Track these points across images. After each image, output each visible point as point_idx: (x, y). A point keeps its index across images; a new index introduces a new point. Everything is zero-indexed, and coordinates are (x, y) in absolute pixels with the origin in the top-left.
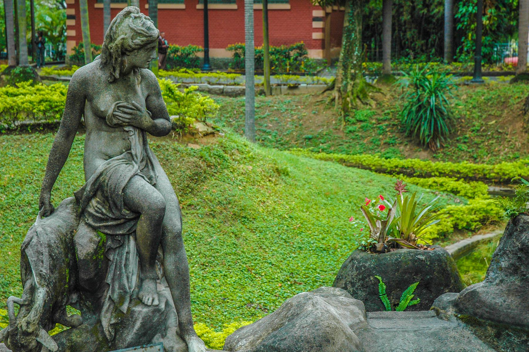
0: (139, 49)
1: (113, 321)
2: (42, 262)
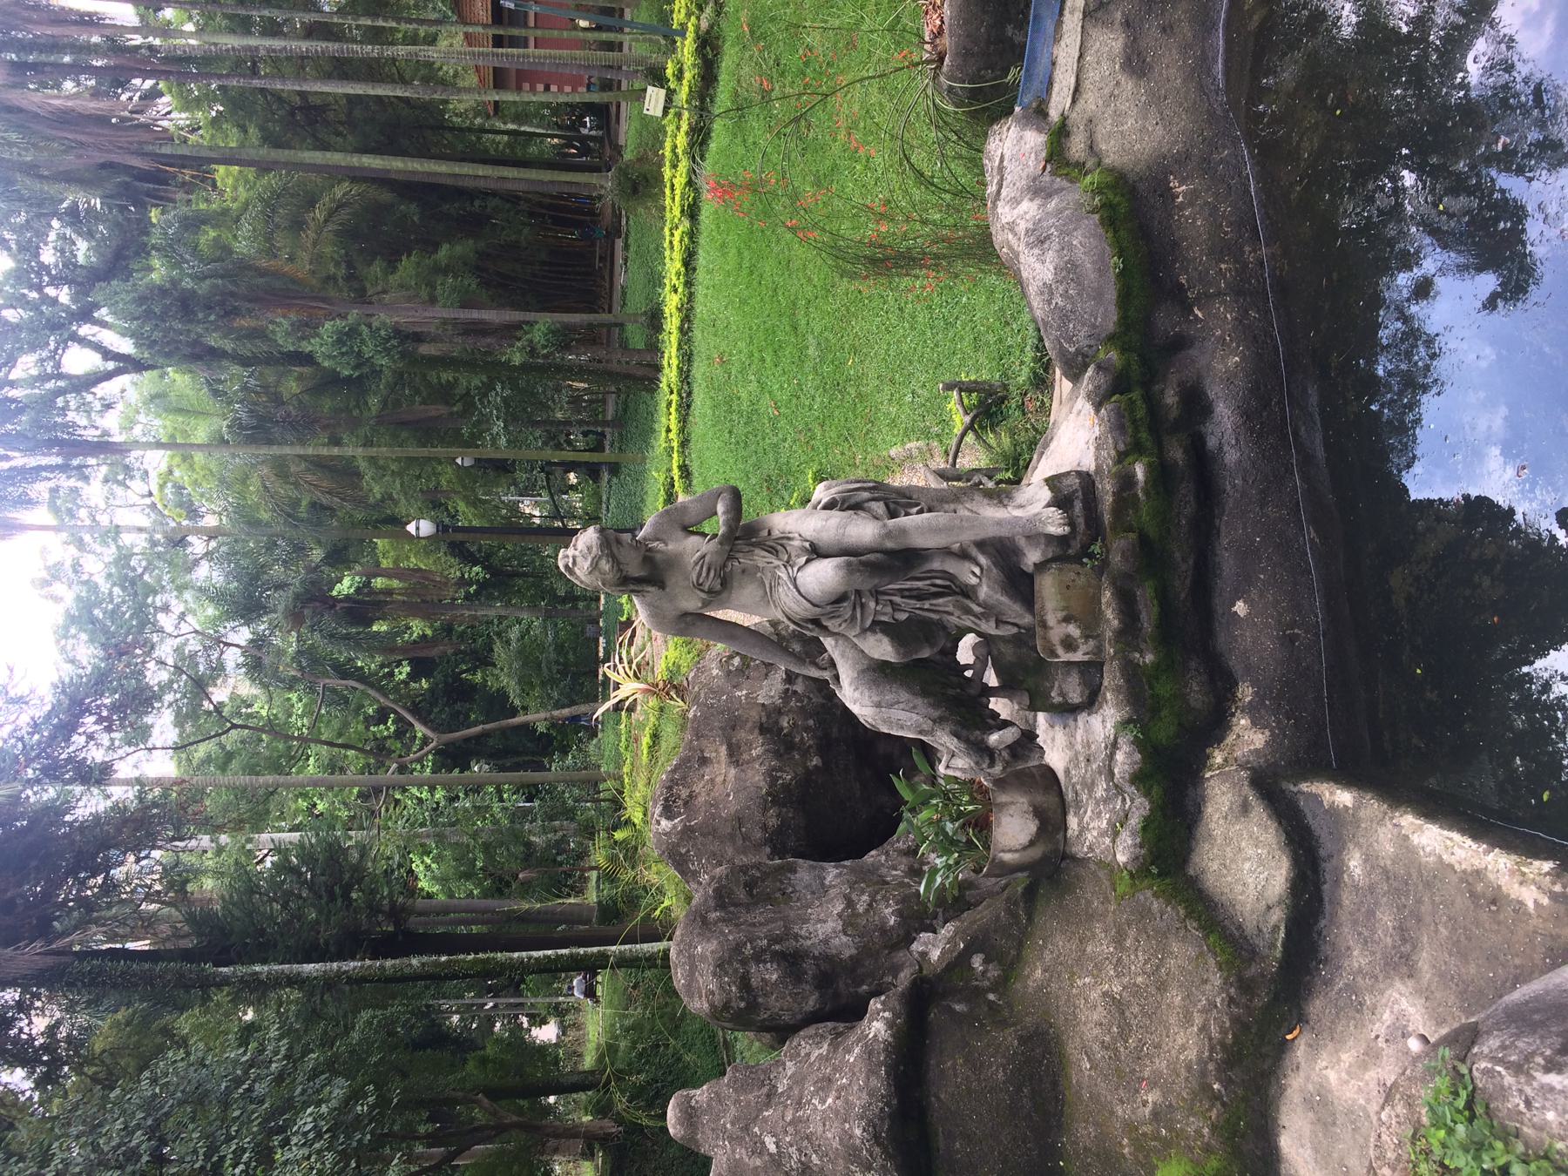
0: (619, 563)
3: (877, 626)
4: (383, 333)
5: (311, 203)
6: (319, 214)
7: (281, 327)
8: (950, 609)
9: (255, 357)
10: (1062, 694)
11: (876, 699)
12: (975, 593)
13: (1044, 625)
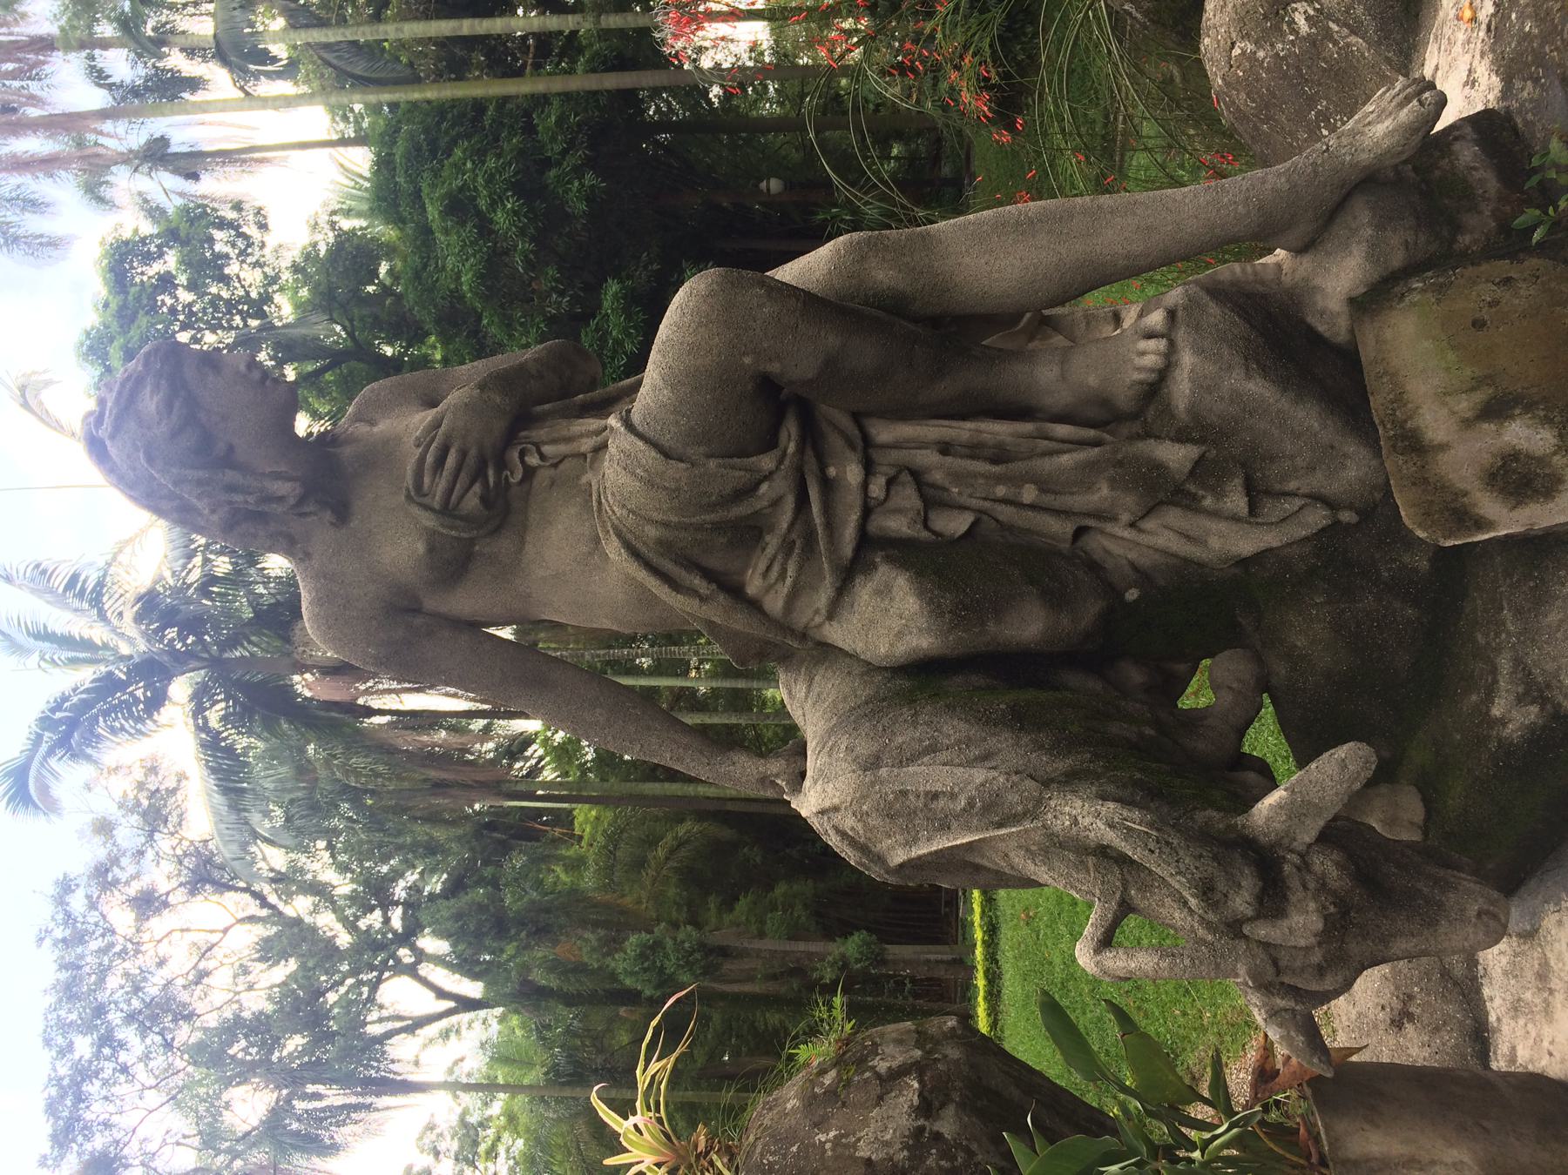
1: (1237, 501)
2: (935, 796)
3: (872, 548)
4: (687, 945)
5: (652, 842)
6: (661, 853)
7: (582, 946)
8: (1102, 493)
9: (579, 995)
10: (1533, 691)
11: (865, 748)
12: (1167, 411)
13: (1414, 444)
